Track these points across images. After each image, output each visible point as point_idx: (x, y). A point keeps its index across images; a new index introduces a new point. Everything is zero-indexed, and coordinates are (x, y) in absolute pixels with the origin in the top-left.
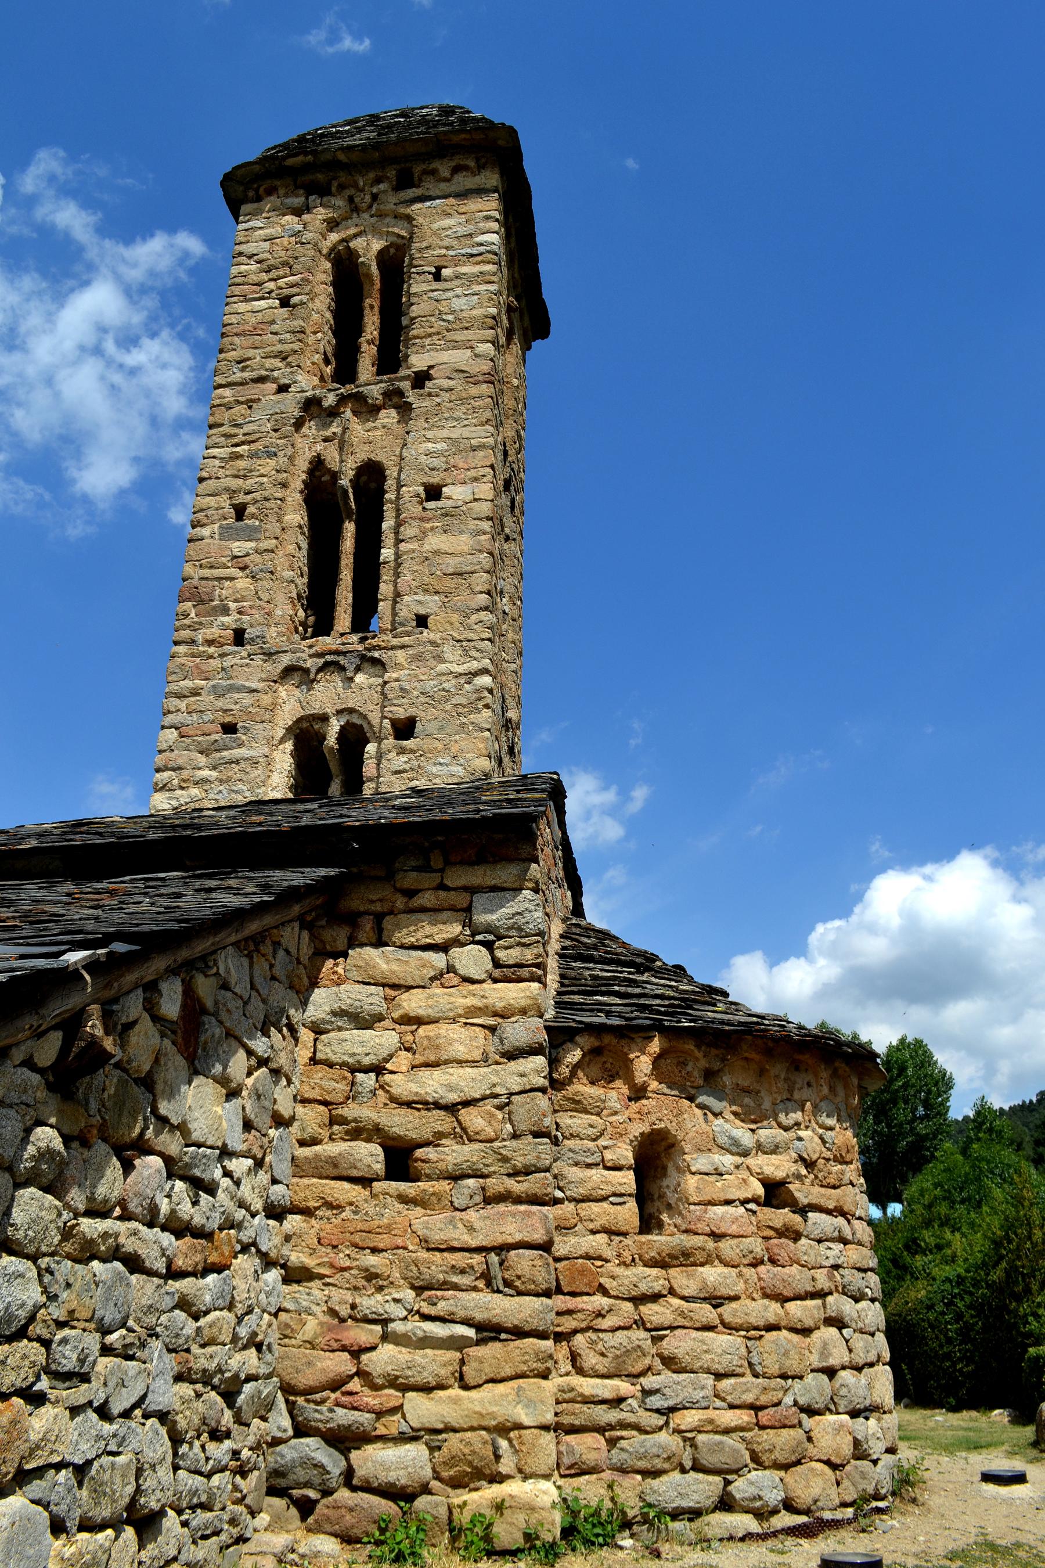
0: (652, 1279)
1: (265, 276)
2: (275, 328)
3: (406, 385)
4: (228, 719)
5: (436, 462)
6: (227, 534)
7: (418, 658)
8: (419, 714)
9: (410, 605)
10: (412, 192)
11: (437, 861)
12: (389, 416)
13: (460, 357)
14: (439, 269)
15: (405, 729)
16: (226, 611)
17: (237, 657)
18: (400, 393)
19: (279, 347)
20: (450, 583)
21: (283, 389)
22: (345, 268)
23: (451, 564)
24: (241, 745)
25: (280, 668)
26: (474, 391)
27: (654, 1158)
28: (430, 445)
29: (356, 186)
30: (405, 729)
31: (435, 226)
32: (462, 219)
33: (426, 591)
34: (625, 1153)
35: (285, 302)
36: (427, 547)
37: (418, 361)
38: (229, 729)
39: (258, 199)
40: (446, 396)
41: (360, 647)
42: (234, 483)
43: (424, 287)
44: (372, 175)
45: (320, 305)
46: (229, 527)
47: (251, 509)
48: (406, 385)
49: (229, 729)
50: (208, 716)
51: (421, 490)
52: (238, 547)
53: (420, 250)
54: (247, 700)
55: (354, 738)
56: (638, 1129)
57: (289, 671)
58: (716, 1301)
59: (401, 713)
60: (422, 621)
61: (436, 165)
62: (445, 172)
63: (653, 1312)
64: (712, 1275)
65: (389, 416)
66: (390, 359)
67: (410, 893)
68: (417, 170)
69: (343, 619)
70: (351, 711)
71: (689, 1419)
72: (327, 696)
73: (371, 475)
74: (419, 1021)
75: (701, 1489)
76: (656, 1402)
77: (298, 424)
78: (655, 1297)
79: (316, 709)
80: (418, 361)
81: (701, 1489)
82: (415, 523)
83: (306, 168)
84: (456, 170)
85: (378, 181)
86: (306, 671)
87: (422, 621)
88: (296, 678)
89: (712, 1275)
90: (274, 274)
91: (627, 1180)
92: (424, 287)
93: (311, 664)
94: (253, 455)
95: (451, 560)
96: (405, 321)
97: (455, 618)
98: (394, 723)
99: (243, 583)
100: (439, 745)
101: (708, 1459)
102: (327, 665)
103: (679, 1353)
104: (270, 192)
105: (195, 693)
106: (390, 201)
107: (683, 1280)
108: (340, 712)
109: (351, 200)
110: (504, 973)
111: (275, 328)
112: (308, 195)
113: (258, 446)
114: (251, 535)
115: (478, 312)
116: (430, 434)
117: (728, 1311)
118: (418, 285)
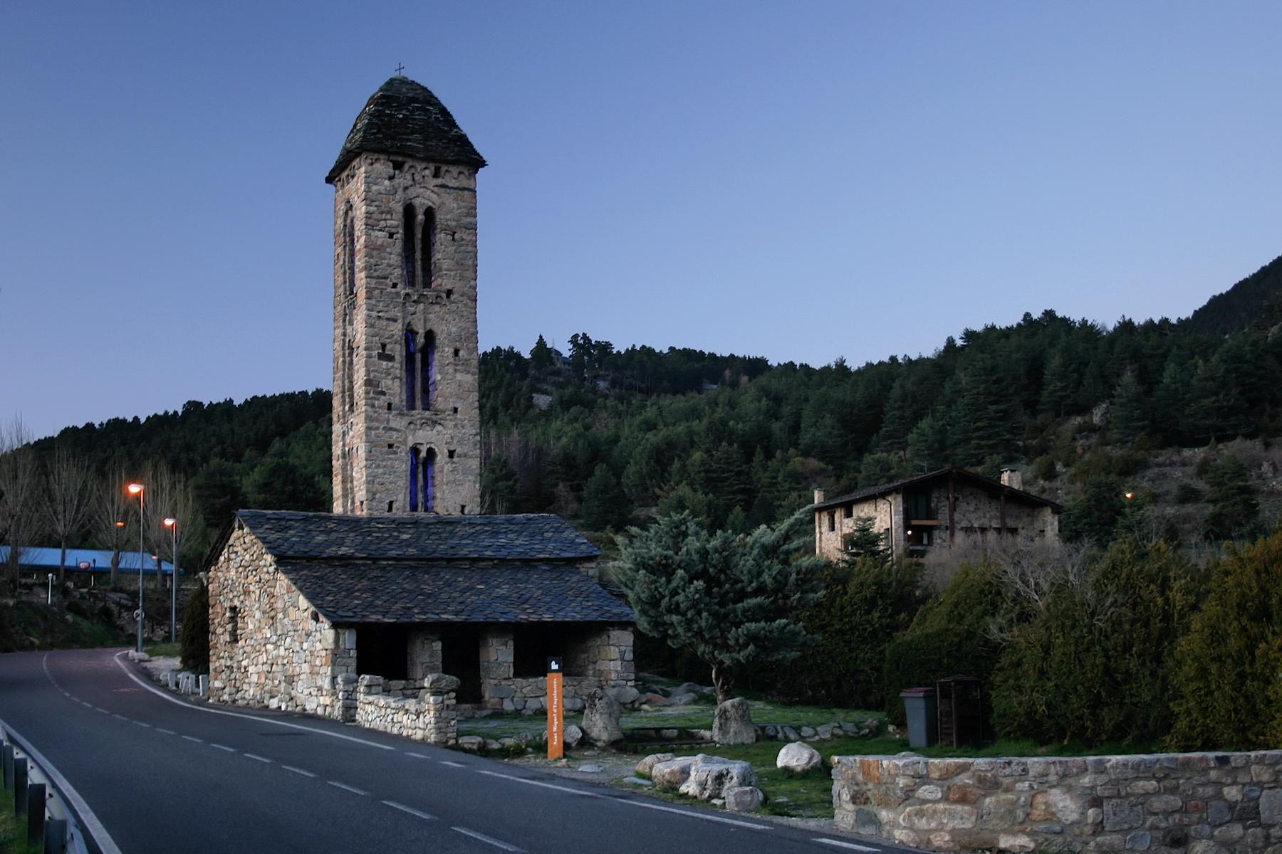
3: (444, 295)
10: (439, 181)
16: (383, 393)
19: (392, 262)
24: (395, 453)
35: (391, 236)
38: (390, 446)
44: (424, 165)
45: (399, 235)
47: (388, 347)
49: (390, 446)
55: (431, 452)
59: (452, 448)
60: (456, 410)
68: (444, 168)
72: (425, 437)
73: (430, 336)
84: (460, 173)
88: (412, 426)
99: (390, 382)
105: (378, 428)
112: (395, 168)
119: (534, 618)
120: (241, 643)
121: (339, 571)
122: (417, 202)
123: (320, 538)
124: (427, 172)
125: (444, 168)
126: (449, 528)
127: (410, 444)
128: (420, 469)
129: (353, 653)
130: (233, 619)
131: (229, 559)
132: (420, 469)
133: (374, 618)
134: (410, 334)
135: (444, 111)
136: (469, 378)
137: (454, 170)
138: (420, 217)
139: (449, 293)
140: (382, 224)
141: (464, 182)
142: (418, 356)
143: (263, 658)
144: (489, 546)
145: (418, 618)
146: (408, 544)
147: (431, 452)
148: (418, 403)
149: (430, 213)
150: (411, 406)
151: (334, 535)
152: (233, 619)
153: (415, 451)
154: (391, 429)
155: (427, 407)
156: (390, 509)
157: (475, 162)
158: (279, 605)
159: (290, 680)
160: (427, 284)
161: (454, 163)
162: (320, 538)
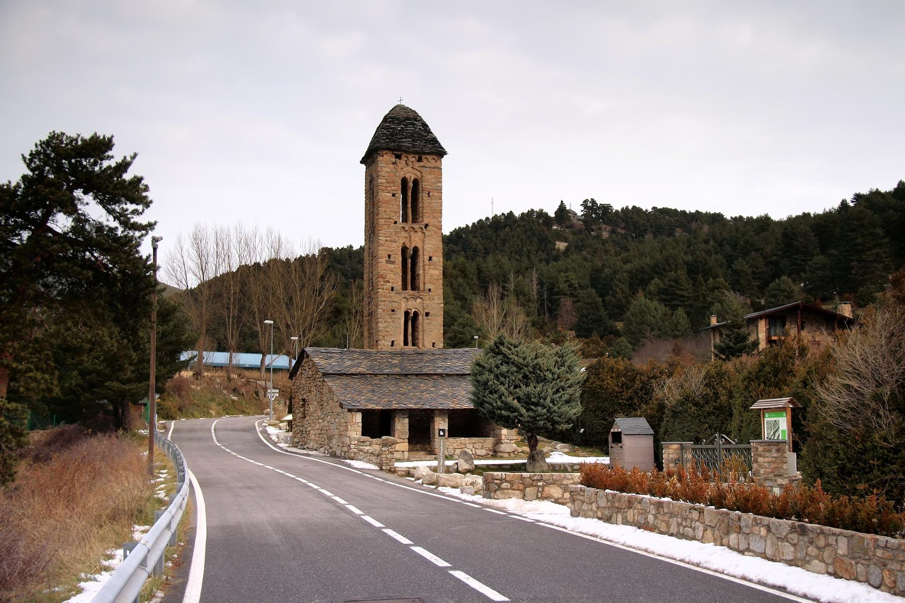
9: (428, 286)
10: (421, 164)
15: (427, 314)
17: (393, 294)
22: (404, 181)
30: (427, 314)
35: (394, 195)
37: (426, 221)
38: (393, 311)
49: (393, 311)
60: (430, 290)
61: (428, 156)
65: (420, 234)
68: (423, 157)
72: (414, 305)
73: (416, 250)
87: (430, 290)
99: (392, 276)
106: (417, 165)
119: (458, 407)
120: (307, 418)
121: (356, 381)
122: (408, 176)
123: (349, 363)
125: (423, 157)
126: (420, 357)
128: (410, 323)
129: (361, 425)
130: (303, 405)
131: (302, 373)
132: (410, 323)
133: (370, 407)
134: (404, 250)
135: (425, 125)
136: (437, 272)
137: (430, 157)
138: (411, 184)
139: (426, 226)
141: (433, 163)
142: (409, 261)
143: (318, 426)
144: (442, 367)
145: (394, 407)
146: (396, 366)
148: (409, 287)
149: (416, 182)
150: (404, 287)
151: (356, 361)
152: (303, 405)
153: (407, 314)
155: (413, 288)
156: (392, 345)
157: (441, 153)
158: (325, 399)
159: (330, 438)
160: (415, 220)
161: (429, 154)
162: (349, 363)
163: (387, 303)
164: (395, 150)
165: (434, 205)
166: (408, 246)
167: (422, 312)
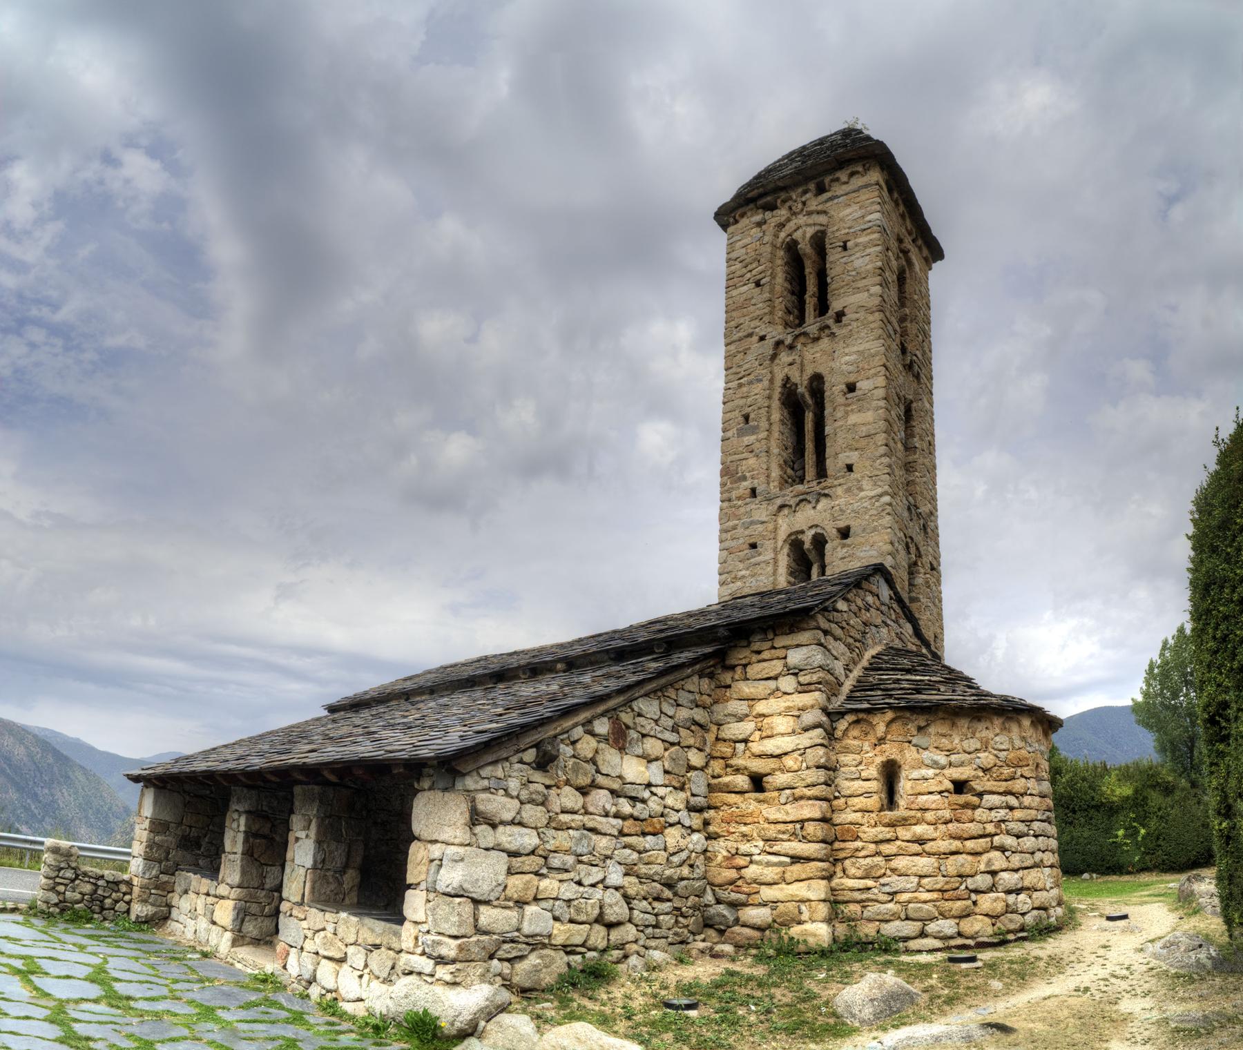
0: (887, 833)
1: (744, 270)
2: (753, 301)
3: (830, 322)
4: (752, 541)
5: (851, 368)
6: (741, 433)
7: (849, 490)
8: (852, 523)
11: (770, 636)
12: (825, 343)
13: (861, 298)
14: (845, 243)
15: (845, 533)
16: (744, 478)
18: (828, 327)
19: (758, 313)
20: (863, 442)
21: (762, 338)
23: (864, 430)
25: (776, 507)
26: (871, 318)
27: (890, 773)
28: (847, 358)
29: (791, 198)
30: (845, 533)
31: (841, 215)
32: (856, 207)
33: (851, 450)
34: (873, 772)
35: (758, 284)
36: (849, 422)
38: (753, 546)
39: (736, 222)
40: (855, 324)
41: (817, 488)
42: (741, 402)
43: (838, 256)
46: (742, 429)
47: (752, 416)
48: (830, 322)
49: (753, 546)
50: (741, 541)
51: (844, 387)
52: (748, 439)
53: (833, 232)
54: (760, 528)
55: (820, 542)
56: (879, 760)
57: (782, 507)
58: (921, 841)
59: (842, 524)
60: (850, 468)
62: (844, 178)
63: (887, 849)
64: (919, 830)
66: (823, 308)
67: (759, 652)
68: (827, 180)
69: (810, 472)
70: (817, 526)
71: (904, 897)
73: (817, 379)
74: (764, 716)
75: (910, 928)
76: (887, 889)
77: (774, 357)
78: (888, 841)
79: (797, 528)
80: (836, 305)
81: (910, 928)
82: (842, 408)
83: (761, 196)
85: (805, 192)
86: (790, 506)
87: (850, 468)
88: (786, 511)
89: (919, 830)
90: (750, 267)
91: (874, 785)
92: (838, 256)
93: (793, 502)
94: (750, 383)
95: (864, 429)
96: (829, 280)
97: (868, 463)
98: (839, 530)
99: (752, 461)
100: (863, 540)
101: (911, 915)
102: (801, 501)
103: (900, 867)
104: (742, 216)
105: (734, 528)
106: (813, 204)
107: (903, 833)
108: (811, 527)
109: (790, 208)
110: (804, 689)
111: (753, 301)
113: (751, 377)
114: (754, 430)
115: (869, 267)
116: (847, 350)
117: (928, 847)
118: (834, 256)
122: (797, 235)
124: (808, 196)
125: (827, 180)
127: (782, 534)
139: (839, 316)
140: (748, 275)
147: (820, 542)
153: (795, 544)
154: (752, 523)
163: (740, 530)
164: (761, 196)
165: (858, 263)
166: (796, 377)
167: (831, 532)
